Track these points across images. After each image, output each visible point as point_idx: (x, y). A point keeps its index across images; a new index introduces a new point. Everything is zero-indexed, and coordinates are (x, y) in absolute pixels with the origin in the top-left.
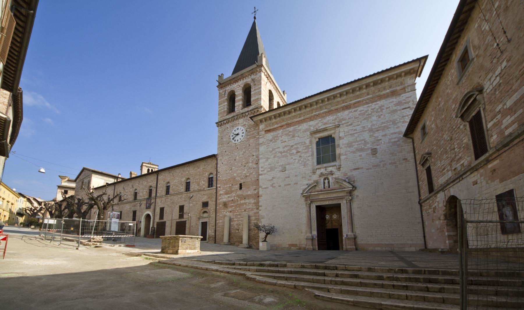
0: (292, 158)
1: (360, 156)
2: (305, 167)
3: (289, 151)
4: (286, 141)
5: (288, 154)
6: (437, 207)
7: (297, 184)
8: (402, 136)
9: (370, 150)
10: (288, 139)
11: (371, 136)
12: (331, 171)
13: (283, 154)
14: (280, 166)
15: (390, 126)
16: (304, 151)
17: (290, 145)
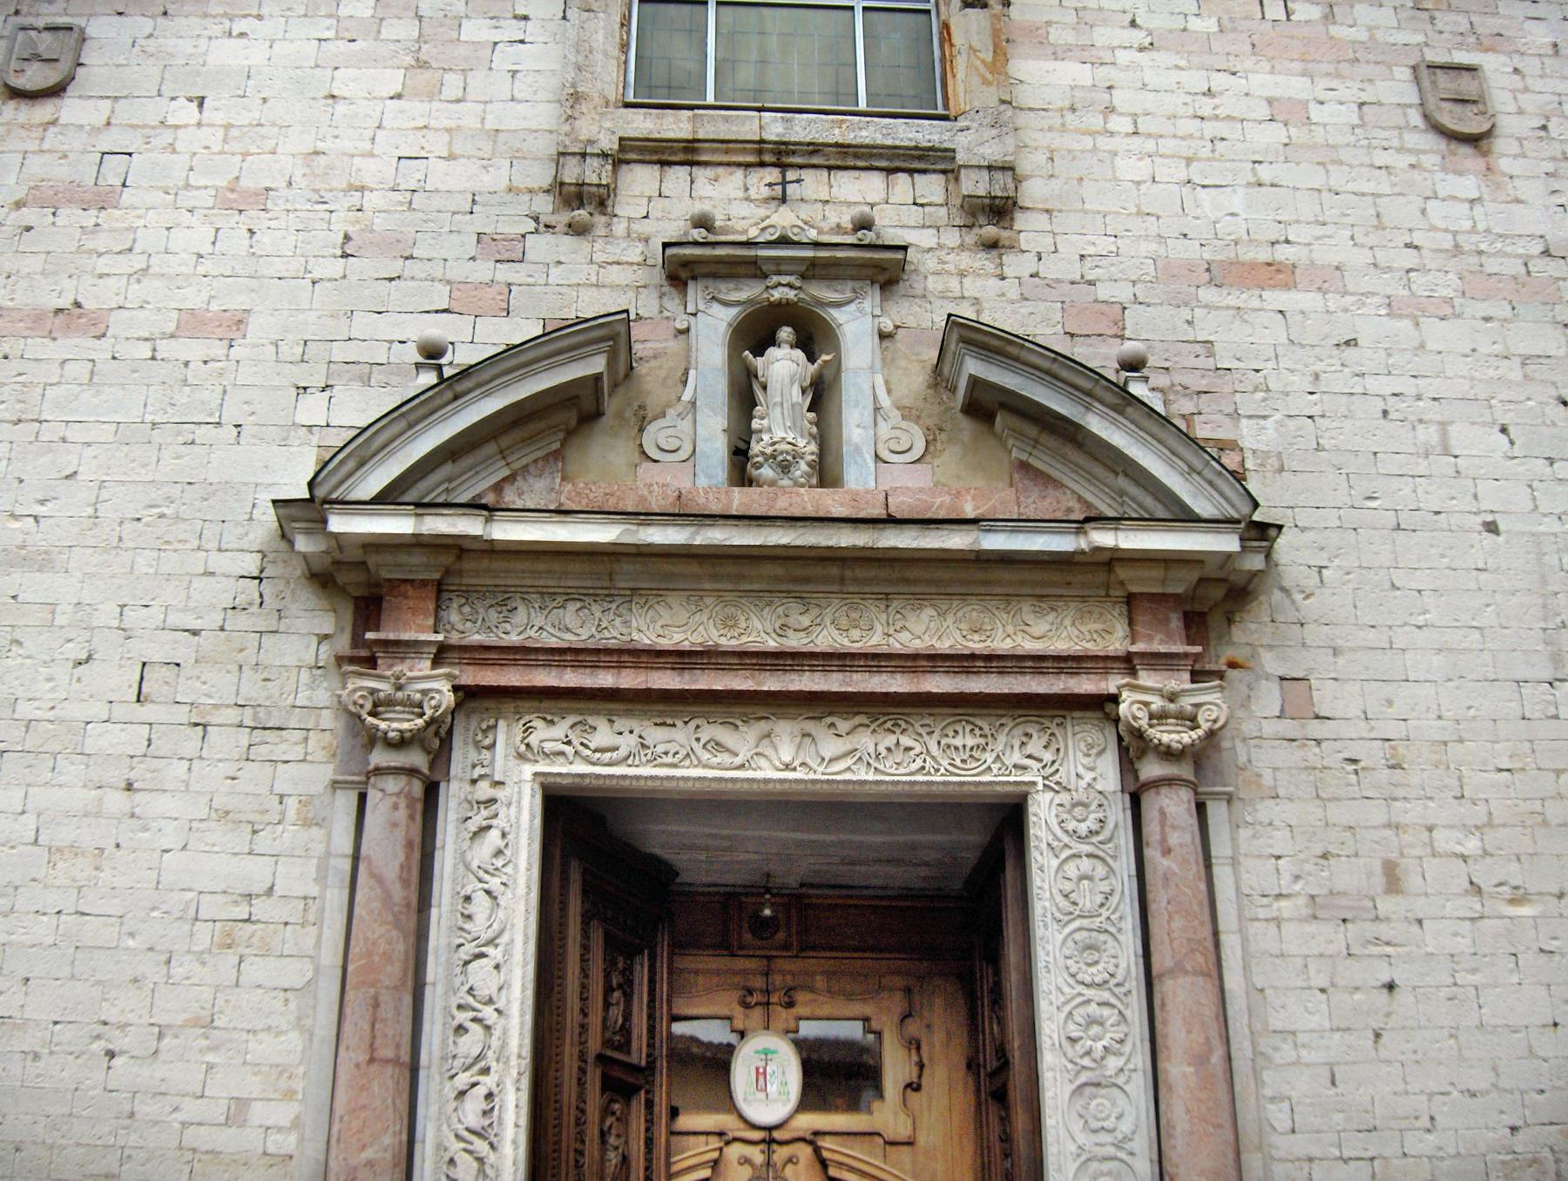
2: (434, 93)
9: (1404, 73)
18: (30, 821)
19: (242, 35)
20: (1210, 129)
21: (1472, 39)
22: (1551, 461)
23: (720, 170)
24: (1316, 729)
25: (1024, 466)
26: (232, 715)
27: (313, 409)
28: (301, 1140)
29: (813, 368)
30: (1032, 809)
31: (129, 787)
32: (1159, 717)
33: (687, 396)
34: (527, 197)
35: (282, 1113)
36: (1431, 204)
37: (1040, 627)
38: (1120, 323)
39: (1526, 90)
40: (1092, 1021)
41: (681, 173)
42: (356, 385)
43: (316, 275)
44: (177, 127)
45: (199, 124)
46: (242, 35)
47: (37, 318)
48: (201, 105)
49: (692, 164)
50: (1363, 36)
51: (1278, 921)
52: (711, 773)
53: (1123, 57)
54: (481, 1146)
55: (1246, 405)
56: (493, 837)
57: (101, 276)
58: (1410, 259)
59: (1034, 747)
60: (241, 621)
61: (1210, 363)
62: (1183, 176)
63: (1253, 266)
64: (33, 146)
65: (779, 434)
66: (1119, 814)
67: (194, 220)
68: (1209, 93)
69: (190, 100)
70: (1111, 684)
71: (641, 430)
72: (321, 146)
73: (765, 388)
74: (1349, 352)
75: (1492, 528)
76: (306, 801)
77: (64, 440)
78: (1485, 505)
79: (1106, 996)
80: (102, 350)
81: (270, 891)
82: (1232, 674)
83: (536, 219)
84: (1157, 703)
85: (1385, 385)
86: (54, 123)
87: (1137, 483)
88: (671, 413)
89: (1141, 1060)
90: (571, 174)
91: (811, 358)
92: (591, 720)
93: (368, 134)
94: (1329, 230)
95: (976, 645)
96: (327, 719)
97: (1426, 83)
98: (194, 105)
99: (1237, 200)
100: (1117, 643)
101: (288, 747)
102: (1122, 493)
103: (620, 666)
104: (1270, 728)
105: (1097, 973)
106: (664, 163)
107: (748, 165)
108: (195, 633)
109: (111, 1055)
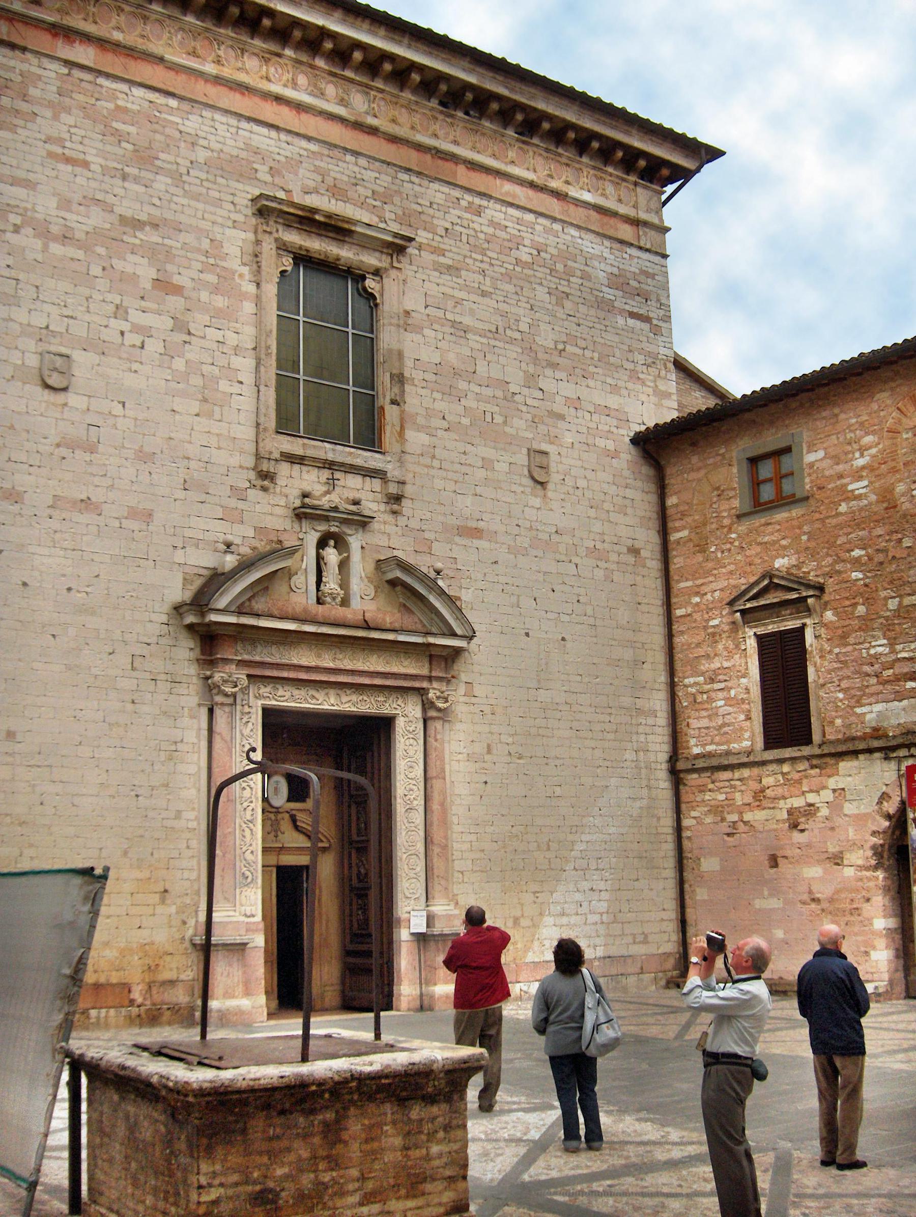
0: (120, 311)
1: (487, 464)
2: (210, 415)
3: (101, 250)
4: (86, 164)
5: (96, 270)
6: (824, 812)
7: (149, 516)
8: (627, 440)
9: (525, 451)
10: (102, 153)
11: (530, 380)
12: (356, 503)
13: (56, 249)
14: (27, 330)
15: (592, 369)
16: (204, 296)
17: (118, 210)
18: (101, 713)
19: (136, 371)
20: (464, 469)
21: (547, 438)
22: (547, 612)
23: (310, 468)
24: (474, 700)
25: (404, 605)
26: (163, 677)
27: (179, 557)
28: (199, 824)
29: (341, 557)
30: (397, 722)
31: (133, 702)
32: (438, 698)
33: (304, 566)
34: (246, 471)
35: (192, 815)
36: (526, 509)
37: (406, 663)
38: (430, 548)
39: (561, 462)
40: (412, 790)
41: (297, 467)
42: (193, 548)
43: (176, 497)
44: (116, 416)
45: (124, 416)
46: (136, 371)
47: (74, 503)
48: (124, 406)
49: (301, 464)
50: (515, 433)
51: (459, 761)
52: (312, 706)
53: (440, 433)
54: (251, 825)
55: (464, 583)
56: (250, 724)
57: (97, 486)
58: (516, 530)
59: (399, 702)
60: (163, 641)
61: (454, 566)
62: (453, 489)
63: (471, 529)
64: (58, 415)
65: (333, 586)
66: (421, 725)
67: (128, 464)
68: (464, 453)
69: (119, 402)
70: (425, 685)
71: (290, 579)
72: (172, 435)
73: (325, 564)
74: (495, 566)
75: (527, 635)
76: (191, 710)
77: (93, 560)
78: (527, 626)
79: (414, 782)
80: (101, 520)
81: (182, 741)
82: (453, 680)
83: (250, 482)
84: (438, 694)
85: (503, 579)
86: (66, 405)
87: (438, 617)
88: (299, 573)
89: (423, 802)
90: (265, 466)
91: (340, 554)
92: (278, 686)
93: (189, 432)
94: (495, 516)
95: (387, 669)
96: (195, 680)
97: (532, 459)
98: (121, 406)
99: (469, 500)
100: (425, 671)
101: (182, 689)
102: (432, 619)
103: (289, 670)
104: (462, 699)
105: (411, 775)
106: (292, 463)
107: (319, 467)
108: (149, 644)
109: (137, 796)
